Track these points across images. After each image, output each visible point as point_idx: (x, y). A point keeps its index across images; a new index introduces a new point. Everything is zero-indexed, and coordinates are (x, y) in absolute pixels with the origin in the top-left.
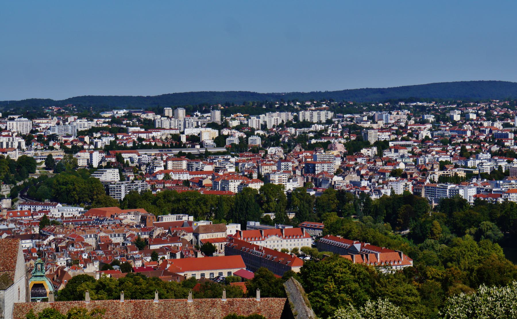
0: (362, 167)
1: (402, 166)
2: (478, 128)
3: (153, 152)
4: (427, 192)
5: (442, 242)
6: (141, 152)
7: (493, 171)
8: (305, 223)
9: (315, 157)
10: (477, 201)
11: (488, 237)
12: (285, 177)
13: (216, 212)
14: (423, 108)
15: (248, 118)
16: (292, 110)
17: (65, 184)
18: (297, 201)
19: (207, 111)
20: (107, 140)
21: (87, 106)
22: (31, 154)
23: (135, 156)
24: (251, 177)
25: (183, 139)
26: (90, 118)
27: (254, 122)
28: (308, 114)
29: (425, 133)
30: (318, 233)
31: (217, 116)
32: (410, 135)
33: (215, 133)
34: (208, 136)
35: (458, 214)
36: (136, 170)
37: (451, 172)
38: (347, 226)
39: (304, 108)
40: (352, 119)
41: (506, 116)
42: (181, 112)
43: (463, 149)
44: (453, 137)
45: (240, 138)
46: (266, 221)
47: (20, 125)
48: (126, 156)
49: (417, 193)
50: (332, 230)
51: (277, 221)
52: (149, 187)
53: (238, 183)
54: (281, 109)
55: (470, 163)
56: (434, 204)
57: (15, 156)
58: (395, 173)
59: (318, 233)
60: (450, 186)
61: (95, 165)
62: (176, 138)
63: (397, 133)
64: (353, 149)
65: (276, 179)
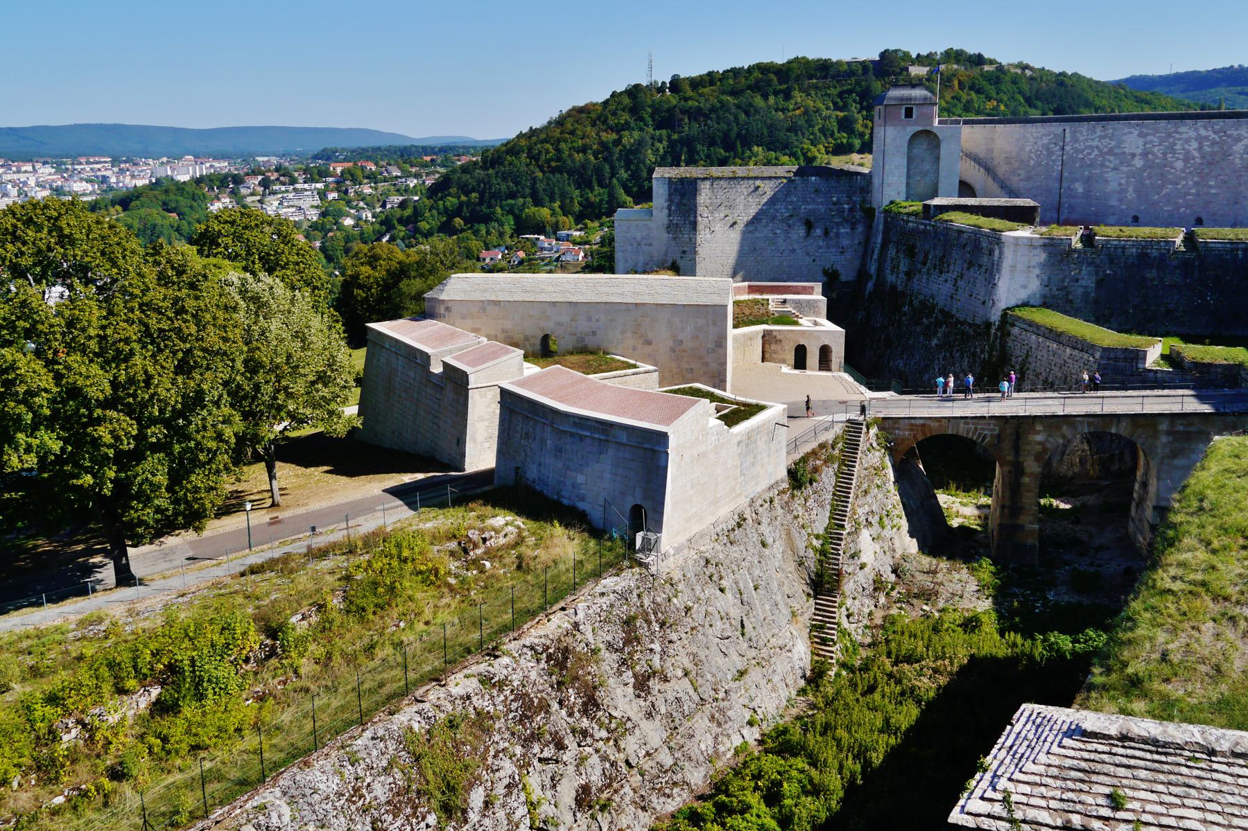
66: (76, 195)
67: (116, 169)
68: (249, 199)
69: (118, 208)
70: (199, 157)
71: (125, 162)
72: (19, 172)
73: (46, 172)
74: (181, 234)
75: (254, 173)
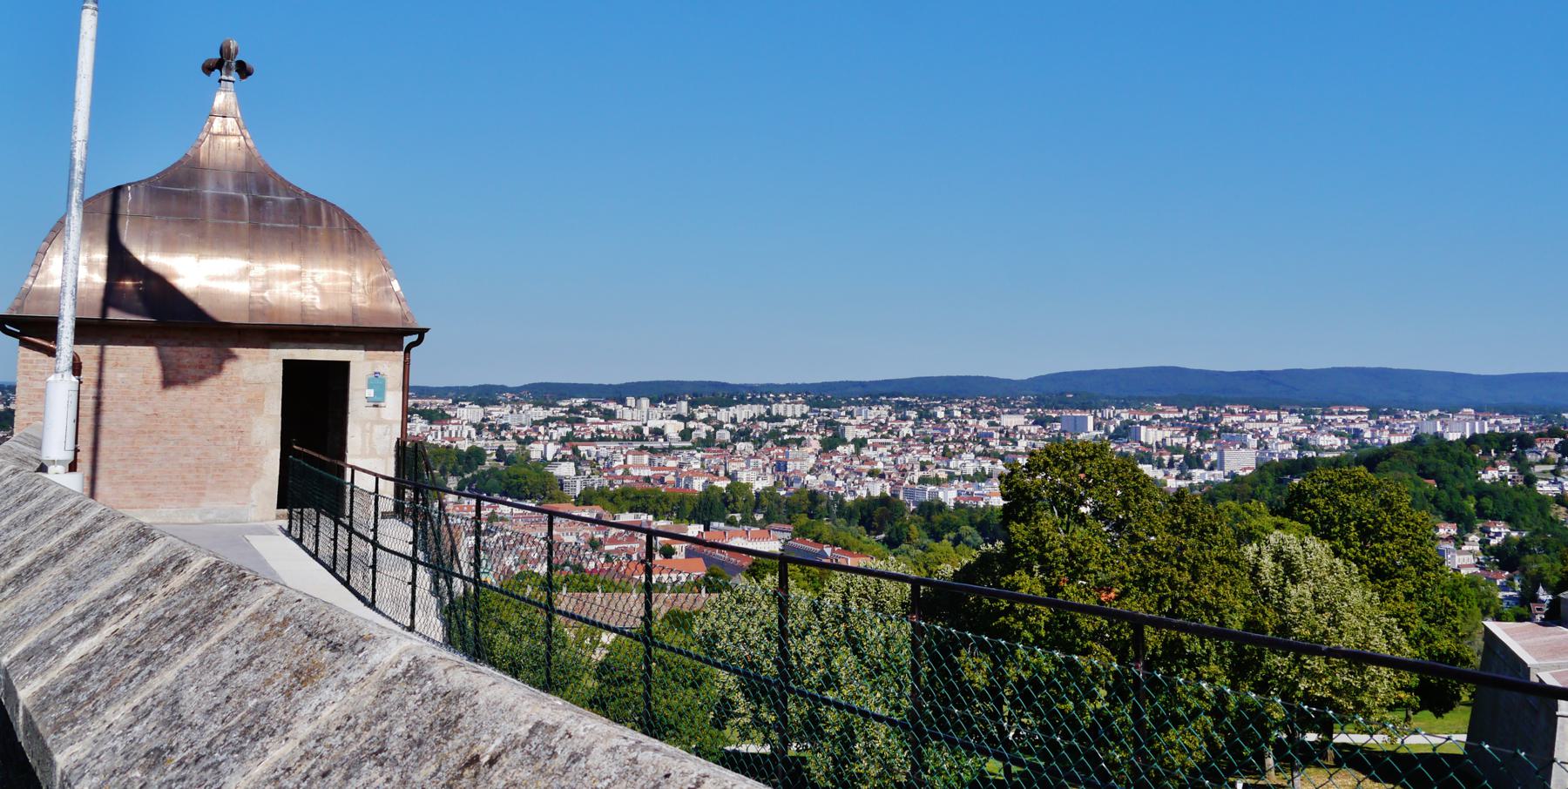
0: (838, 465)
1: (880, 466)
2: (963, 426)
3: (613, 445)
4: (905, 494)
5: (918, 547)
6: (599, 444)
7: (976, 473)
8: (774, 525)
9: (787, 454)
10: (957, 505)
11: (968, 543)
12: (754, 475)
13: (678, 511)
14: (906, 405)
15: (717, 410)
16: (765, 403)
17: (517, 477)
18: (765, 502)
19: (673, 402)
20: (564, 431)
21: (544, 394)
22: (480, 444)
23: (593, 449)
24: (717, 474)
25: (646, 432)
26: (547, 406)
27: (723, 415)
28: (781, 407)
29: (906, 430)
30: (787, 535)
31: (683, 407)
32: (891, 432)
33: (681, 426)
34: (673, 428)
35: (937, 518)
36: (594, 464)
37: (931, 472)
38: (817, 529)
39: (778, 400)
40: (829, 414)
41: (992, 414)
42: (645, 402)
43: (946, 449)
44: (935, 435)
45: (708, 432)
46: (731, 523)
47: (471, 413)
48: (583, 449)
49: (895, 495)
50: (802, 533)
51: (743, 522)
52: (606, 483)
53: (703, 480)
54: (753, 401)
55: (953, 464)
56: (912, 507)
57: (464, 446)
58: (871, 474)
59: (787, 535)
60: (930, 488)
61: (549, 458)
62: (638, 430)
63: (877, 430)
64: (829, 446)
65: (743, 477)
66: (1321, 449)
67: (1373, 422)
68: (1538, 469)
69: (1363, 468)
70: (1481, 410)
71: (1386, 414)
72: (1262, 420)
73: (1292, 422)
74: (1438, 507)
75: (1552, 434)
